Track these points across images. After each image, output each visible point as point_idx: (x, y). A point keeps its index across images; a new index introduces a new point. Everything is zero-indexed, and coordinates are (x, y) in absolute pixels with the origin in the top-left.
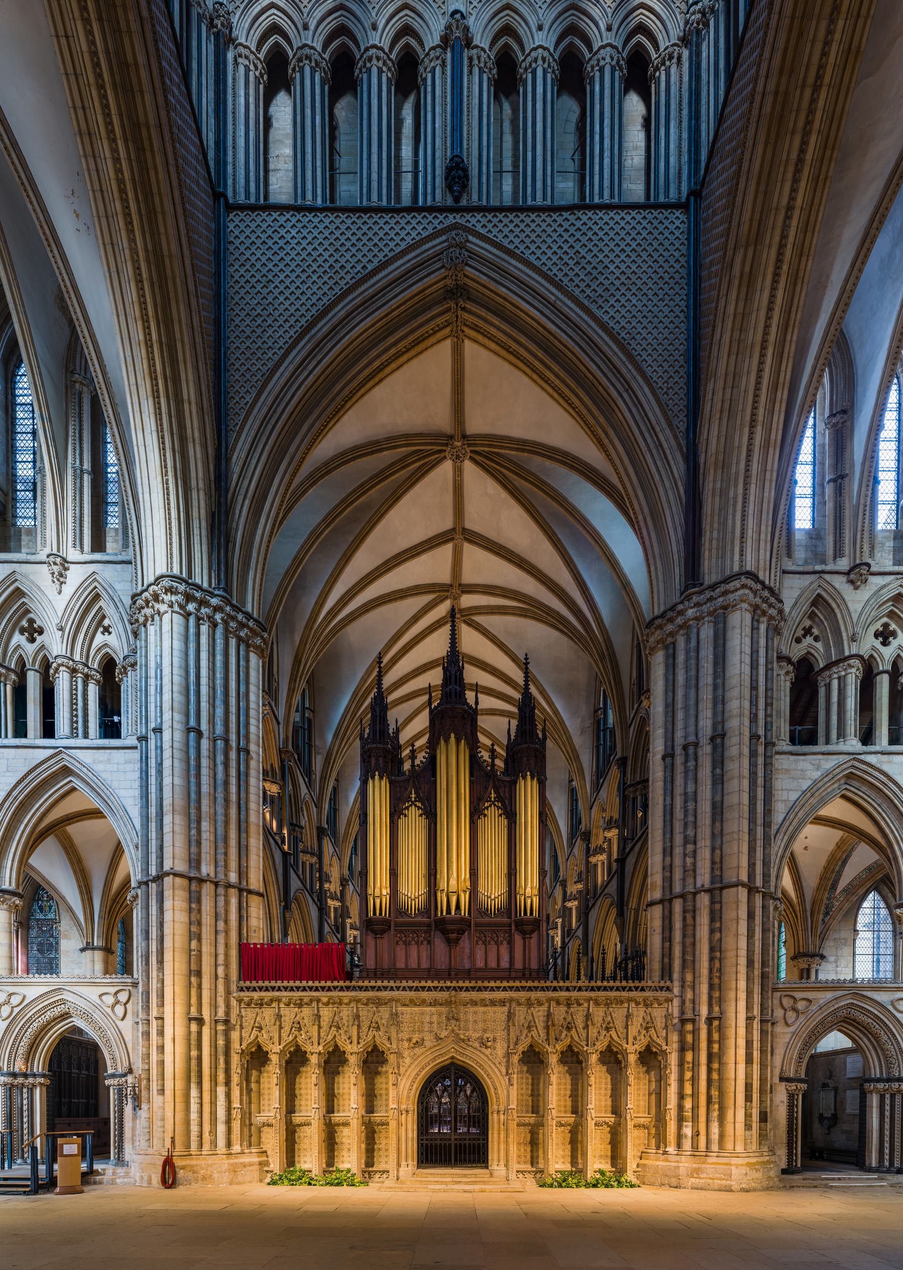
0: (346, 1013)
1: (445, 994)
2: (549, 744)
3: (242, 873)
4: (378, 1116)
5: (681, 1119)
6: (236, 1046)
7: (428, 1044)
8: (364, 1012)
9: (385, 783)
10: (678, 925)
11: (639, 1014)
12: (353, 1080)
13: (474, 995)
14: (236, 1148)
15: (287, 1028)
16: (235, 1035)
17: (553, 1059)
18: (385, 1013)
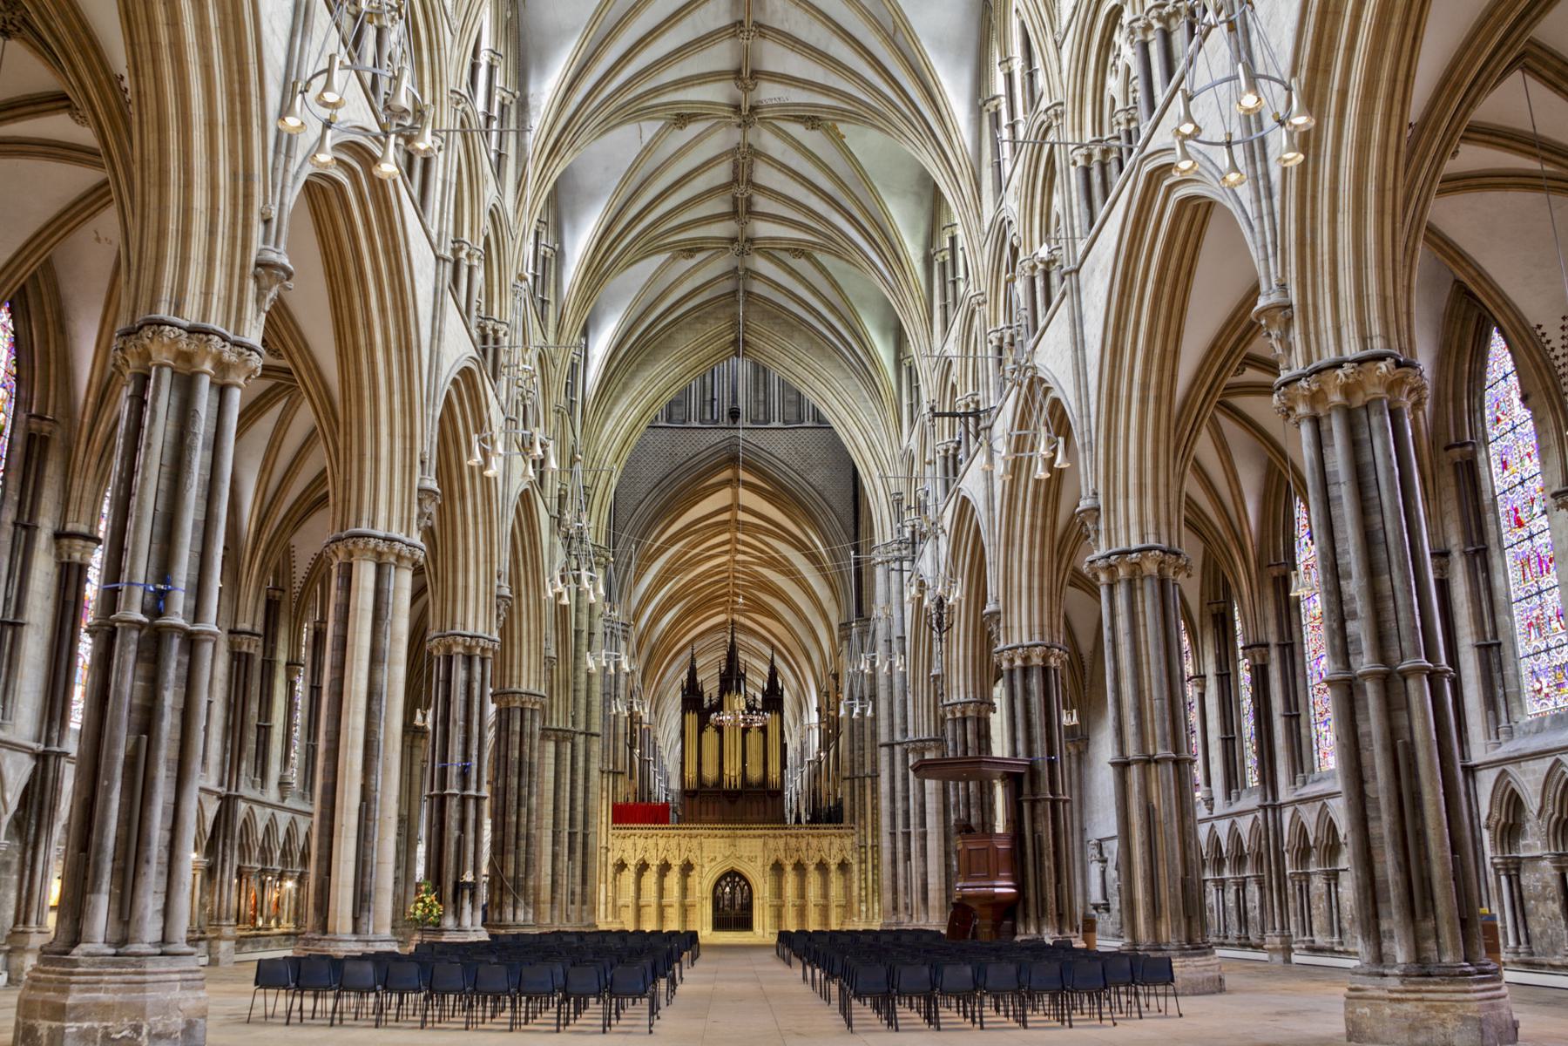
0: (673, 842)
1: (726, 833)
2: (785, 692)
3: (615, 763)
4: (689, 901)
5: (860, 901)
6: (610, 862)
7: (719, 860)
8: (684, 842)
9: (696, 716)
10: (857, 793)
11: (837, 842)
12: (676, 880)
13: (745, 832)
14: (610, 919)
15: (639, 851)
16: (610, 854)
17: (789, 868)
18: (695, 842)
